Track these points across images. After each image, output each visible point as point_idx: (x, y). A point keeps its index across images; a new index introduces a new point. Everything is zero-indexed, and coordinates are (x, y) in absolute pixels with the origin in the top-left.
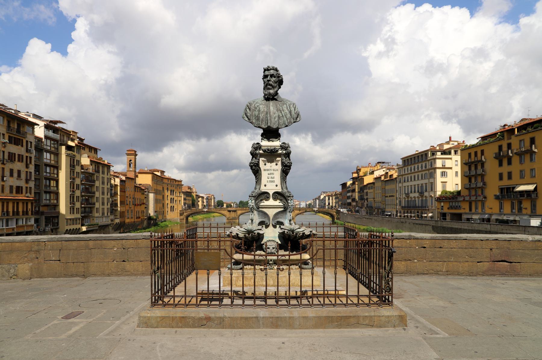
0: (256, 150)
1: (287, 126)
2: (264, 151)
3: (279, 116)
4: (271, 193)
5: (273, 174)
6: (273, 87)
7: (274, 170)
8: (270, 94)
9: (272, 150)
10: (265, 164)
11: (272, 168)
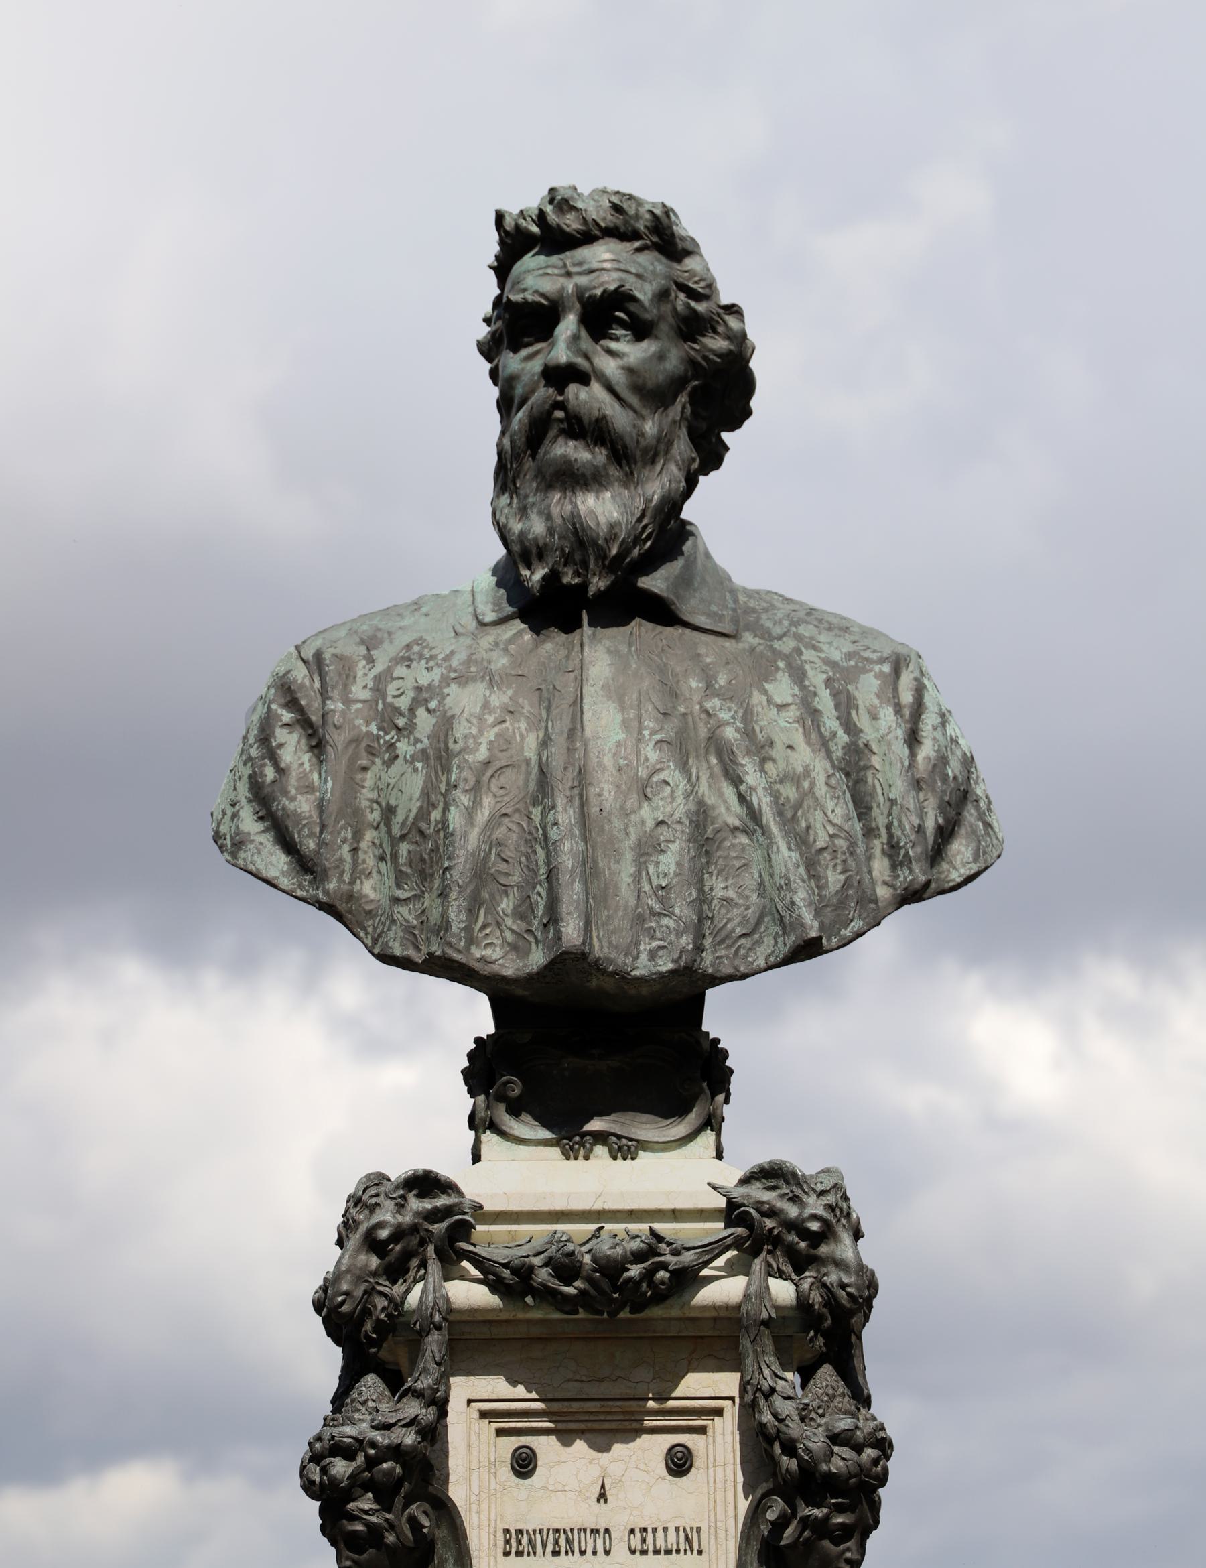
0: (396, 1271)
1: (808, 949)
2: (512, 1281)
3: (701, 817)
6: (626, 457)
8: (580, 542)
9: (610, 1269)
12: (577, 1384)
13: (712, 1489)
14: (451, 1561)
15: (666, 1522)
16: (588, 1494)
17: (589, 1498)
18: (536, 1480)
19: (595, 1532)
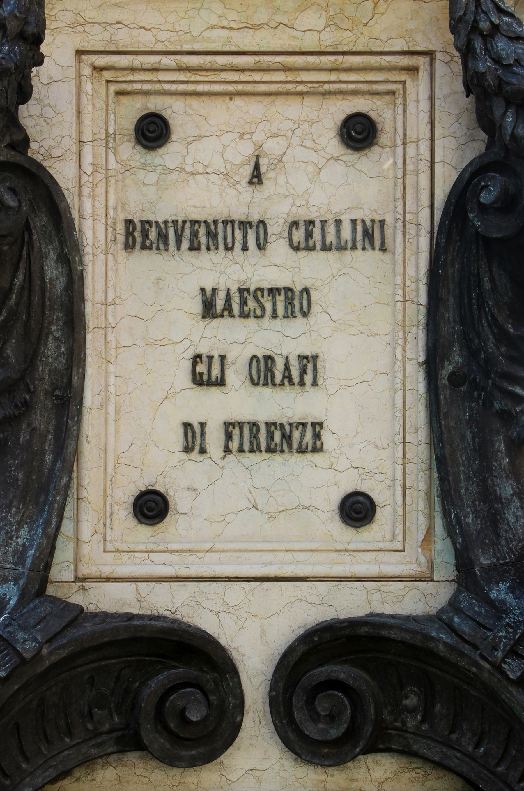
4: (256, 637)
5: (294, 302)
7: (307, 236)
10: (152, 132)
11: (276, 205)
12: (225, 33)
13: (400, 174)
14: (53, 256)
15: (340, 214)
16: (237, 178)
17: (237, 182)
18: (170, 154)
19: (245, 224)
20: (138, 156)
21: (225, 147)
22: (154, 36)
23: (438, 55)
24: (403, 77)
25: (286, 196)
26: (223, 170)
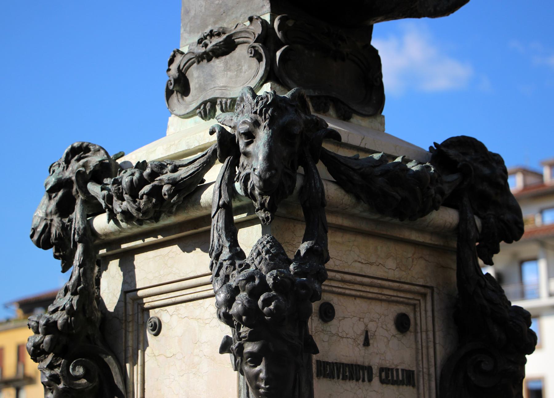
12: (360, 264)
15: (397, 365)
16: (359, 342)
17: (359, 344)
20: (320, 325)
21: (354, 324)
22: (334, 262)
23: (435, 289)
24: (419, 298)
25: (377, 354)
26: (353, 337)
